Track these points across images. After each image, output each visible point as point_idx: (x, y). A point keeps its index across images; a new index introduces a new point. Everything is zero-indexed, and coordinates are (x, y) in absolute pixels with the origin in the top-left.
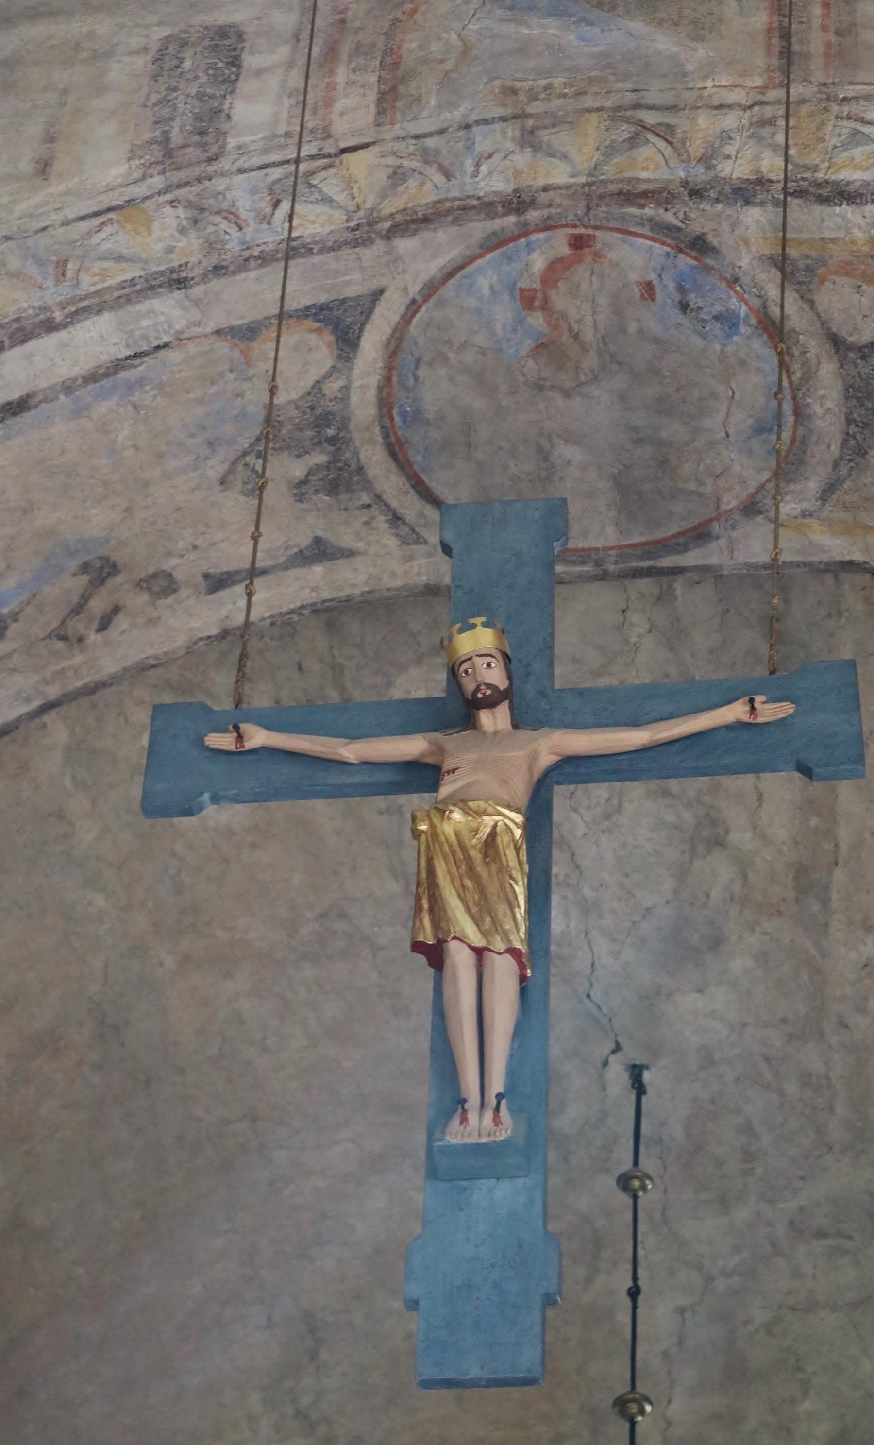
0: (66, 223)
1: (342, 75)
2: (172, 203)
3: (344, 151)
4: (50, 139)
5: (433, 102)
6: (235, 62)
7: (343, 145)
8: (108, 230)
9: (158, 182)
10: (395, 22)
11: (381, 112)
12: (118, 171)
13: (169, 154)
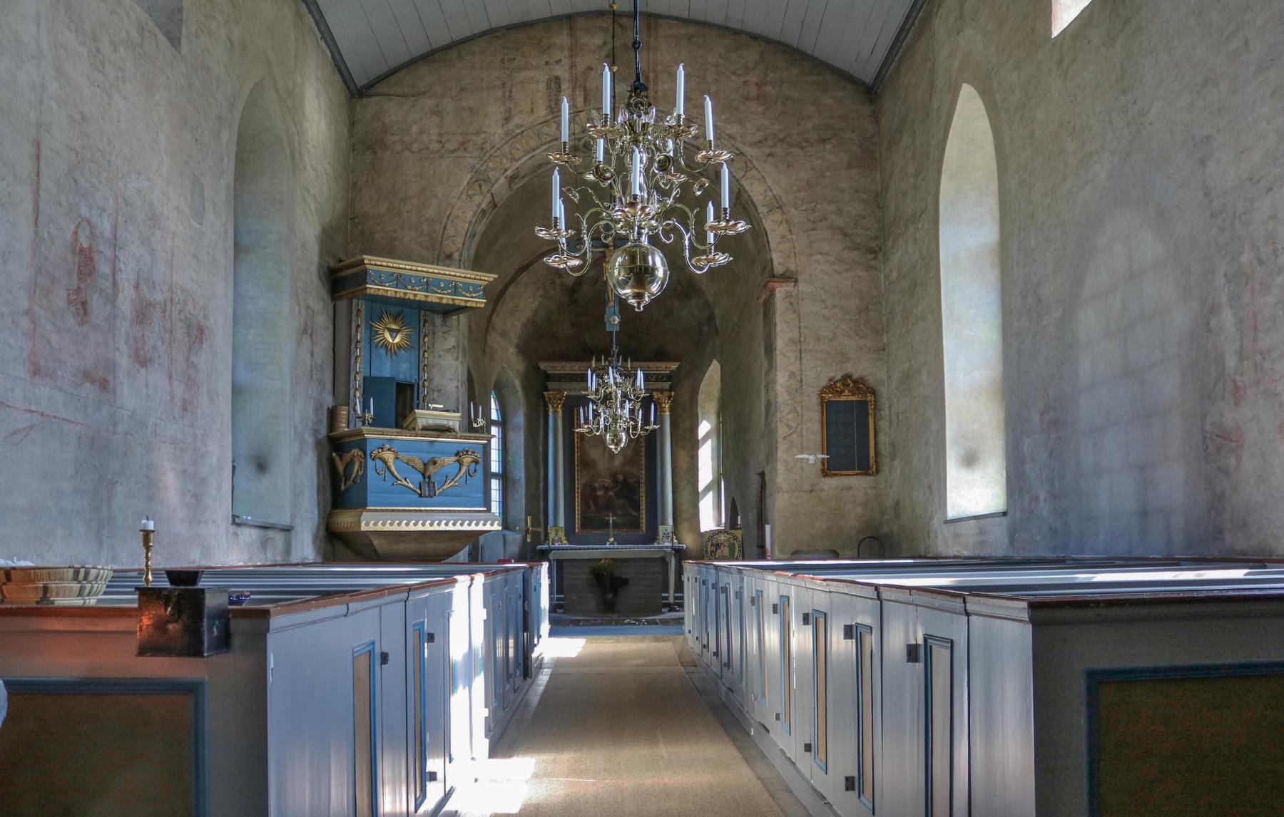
0: (538, 125)
1: (578, 93)
2: (554, 122)
3: (580, 112)
4: (532, 104)
5: (592, 101)
6: (560, 87)
7: (580, 110)
8: (544, 128)
9: (550, 116)
10: (585, 80)
11: (585, 102)
12: (544, 112)
13: (552, 109)
